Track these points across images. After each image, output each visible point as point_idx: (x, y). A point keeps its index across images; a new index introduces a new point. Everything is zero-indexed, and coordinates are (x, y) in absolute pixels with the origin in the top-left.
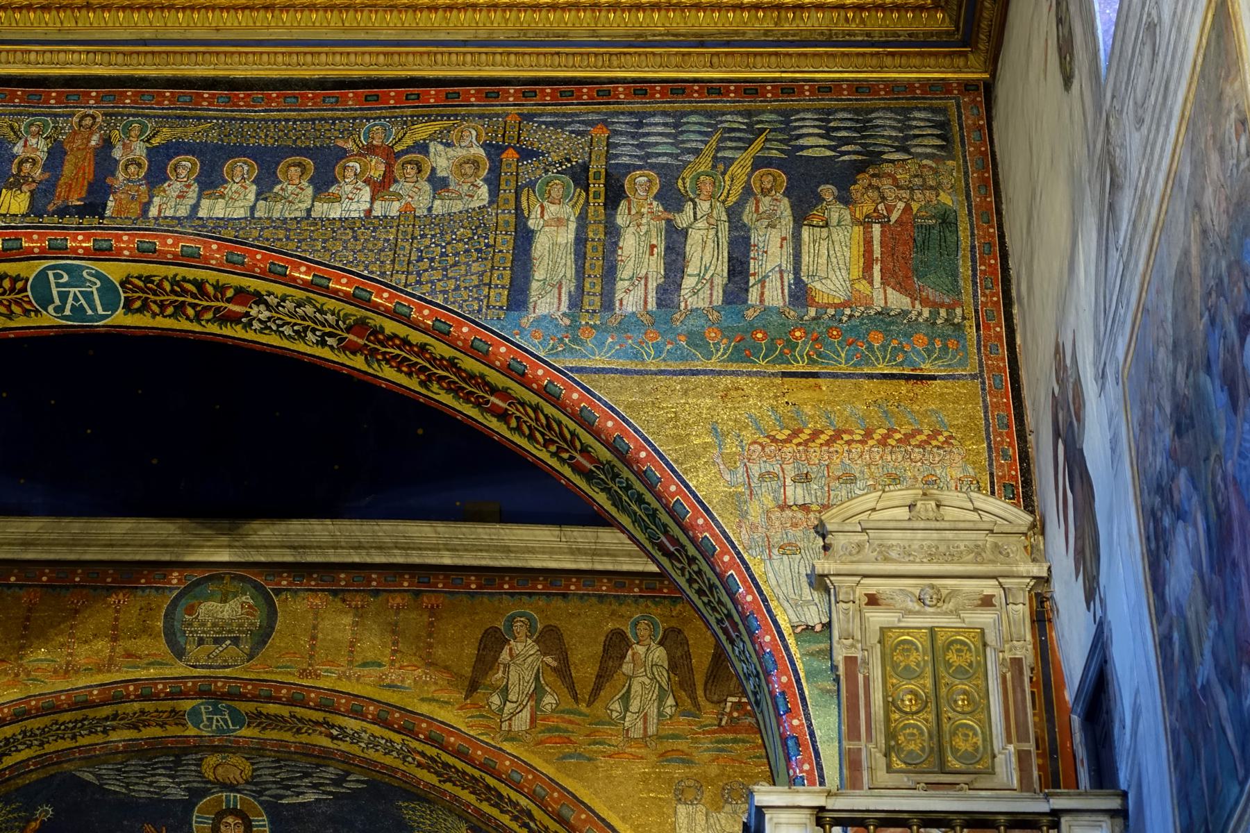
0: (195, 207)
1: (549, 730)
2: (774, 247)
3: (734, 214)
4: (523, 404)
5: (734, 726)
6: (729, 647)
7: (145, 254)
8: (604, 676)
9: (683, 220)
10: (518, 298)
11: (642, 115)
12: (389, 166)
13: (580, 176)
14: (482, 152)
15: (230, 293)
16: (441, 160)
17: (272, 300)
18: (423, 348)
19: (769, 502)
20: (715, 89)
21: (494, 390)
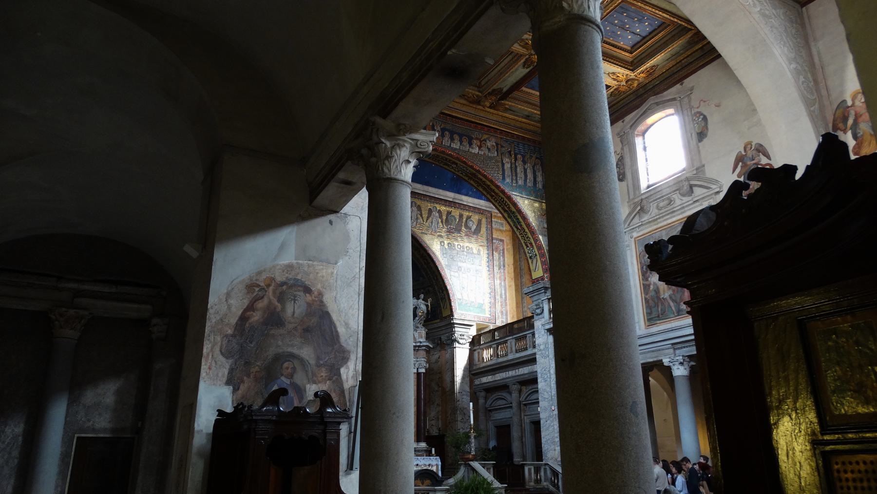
0: (450, 144)
1: (420, 227)
2: (540, 177)
3: (533, 167)
4: (499, 196)
5: (449, 232)
6: (525, 247)
7: (443, 152)
8: (428, 218)
9: (526, 167)
10: (504, 178)
11: (519, 143)
12: (481, 143)
13: (510, 152)
14: (494, 144)
15: (451, 162)
16: (489, 144)
17: (458, 165)
18: (484, 181)
19: (542, 227)
20: (529, 140)
21: (494, 192)
